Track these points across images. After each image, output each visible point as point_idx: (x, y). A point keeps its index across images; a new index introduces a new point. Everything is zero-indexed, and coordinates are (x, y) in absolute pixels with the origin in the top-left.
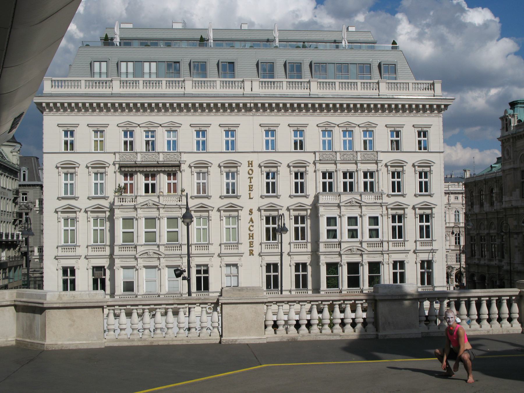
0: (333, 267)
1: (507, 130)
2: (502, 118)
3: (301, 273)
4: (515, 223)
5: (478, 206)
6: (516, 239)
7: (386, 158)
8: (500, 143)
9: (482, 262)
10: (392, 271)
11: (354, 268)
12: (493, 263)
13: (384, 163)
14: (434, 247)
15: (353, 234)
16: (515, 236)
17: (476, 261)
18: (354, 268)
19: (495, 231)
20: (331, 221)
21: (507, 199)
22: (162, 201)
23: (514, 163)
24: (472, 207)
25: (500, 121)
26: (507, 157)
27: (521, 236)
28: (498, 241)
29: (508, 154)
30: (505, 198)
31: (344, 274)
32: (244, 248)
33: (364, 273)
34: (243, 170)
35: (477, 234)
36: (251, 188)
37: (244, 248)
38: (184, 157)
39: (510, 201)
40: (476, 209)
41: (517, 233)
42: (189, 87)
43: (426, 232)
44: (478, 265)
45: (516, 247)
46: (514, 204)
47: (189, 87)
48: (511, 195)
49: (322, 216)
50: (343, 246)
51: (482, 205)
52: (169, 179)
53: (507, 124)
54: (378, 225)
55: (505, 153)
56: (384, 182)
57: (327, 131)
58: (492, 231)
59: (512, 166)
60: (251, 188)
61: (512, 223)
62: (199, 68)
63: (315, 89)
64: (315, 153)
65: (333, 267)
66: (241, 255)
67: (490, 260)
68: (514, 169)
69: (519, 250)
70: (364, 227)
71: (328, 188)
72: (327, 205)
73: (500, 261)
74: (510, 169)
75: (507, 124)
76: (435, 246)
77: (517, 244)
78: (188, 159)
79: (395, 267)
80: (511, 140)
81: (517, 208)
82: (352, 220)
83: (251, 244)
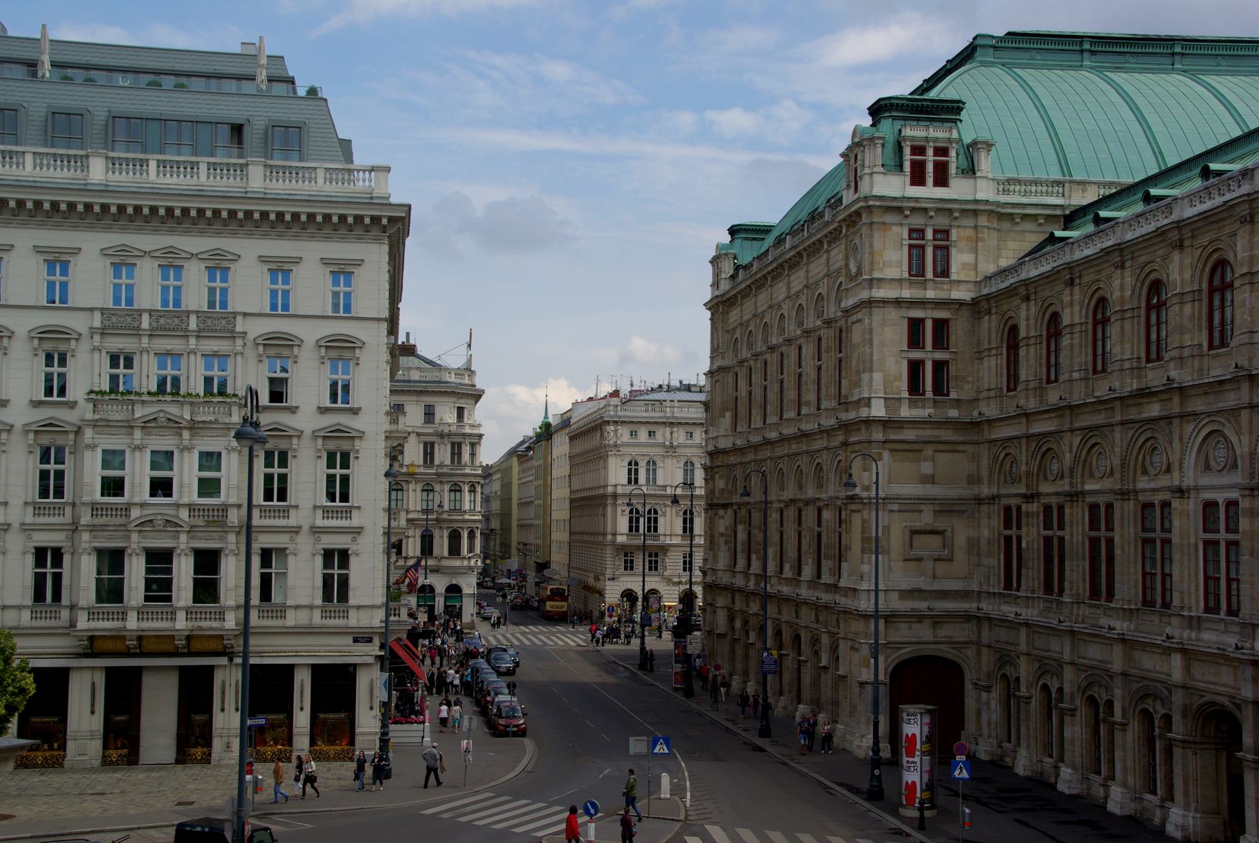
0: (113, 560)
11: (159, 560)
13: (251, 336)
14: (356, 521)
15: (161, 487)
16: (721, 512)
18: (159, 560)
27: (730, 511)
31: (135, 573)
33: (184, 572)
43: (339, 490)
45: (722, 535)
49: (93, 447)
50: (135, 513)
54: (171, 469)
57: (122, 262)
64: (92, 310)
69: (726, 542)
70: (186, 474)
77: (722, 530)
82: (163, 459)
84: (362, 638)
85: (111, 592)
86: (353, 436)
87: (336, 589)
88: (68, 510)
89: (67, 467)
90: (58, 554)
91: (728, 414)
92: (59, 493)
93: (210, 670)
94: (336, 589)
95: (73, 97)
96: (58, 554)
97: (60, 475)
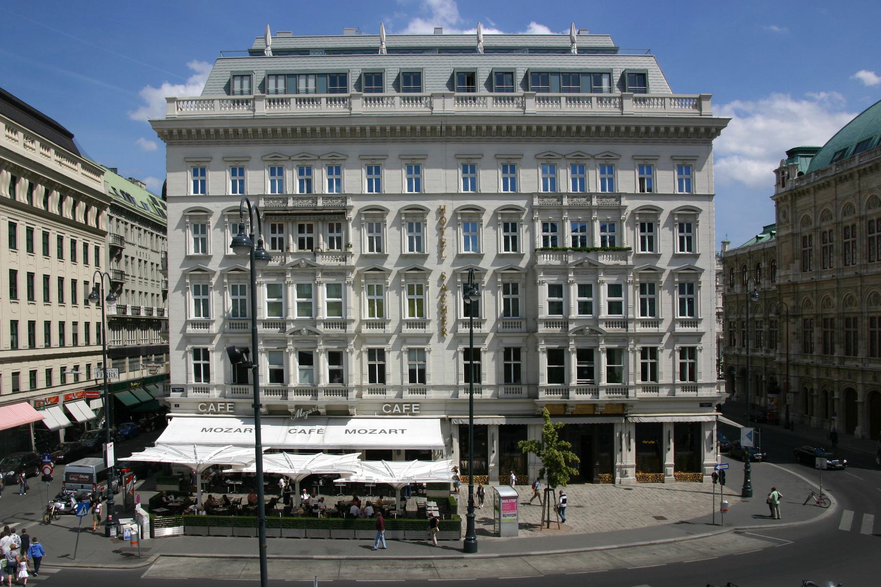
1: (783, 186)
2: (776, 171)
3: (512, 362)
4: (791, 303)
5: (739, 285)
6: (794, 323)
7: (631, 205)
8: (774, 203)
9: (744, 353)
10: (639, 361)
12: (758, 354)
16: (792, 320)
17: (736, 352)
19: (762, 315)
20: (556, 290)
21: (783, 273)
22: (321, 261)
23: (793, 228)
24: (732, 285)
25: (774, 175)
26: (783, 220)
27: (800, 319)
28: (765, 328)
29: (784, 216)
30: (780, 273)
32: (432, 328)
34: (431, 221)
35: (738, 320)
36: (441, 244)
37: (432, 328)
38: (350, 202)
39: (787, 276)
40: (738, 289)
41: (795, 316)
42: (359, 107)
44: (738, 357)
46: (791, 278)
47: (359, 107)
48: (788, 269)
49: (543, 283)
51: (744, 284)
52: (331, 231)
53: (783, 179)
55: (781, 214)
56: (630, 237)
58: (757, 316)
59: (790, 231)
60: (441, 244)
61: (789, 302)
62: (372, 81)
63: (533, 107)
65: (556, 357)
66: (428, 337)
67: (754, 351)
68: (793, 235)
71: (552, 246)
72: (548, 270)
73: (768, 352)
74: (787, 235)
75: (783, 179)
76: (701, 328)
78: (355, 206)
79: (644, 357)
80: (790, 198)
81: (795, 284)
82: (585, 290)
83: (443, 321)
84: (705, 404)
85: (557, 375)
86: (699, 272)
87: (688, 372)
88: (523, 323)
89: (520, 296)
90: (517, 351)
91: (798, 263)
92: (516, 313)
93: (611, 426)
94: (688, 372)
95: (503, 62)
96: (517, 351)
97: (516, 301)
